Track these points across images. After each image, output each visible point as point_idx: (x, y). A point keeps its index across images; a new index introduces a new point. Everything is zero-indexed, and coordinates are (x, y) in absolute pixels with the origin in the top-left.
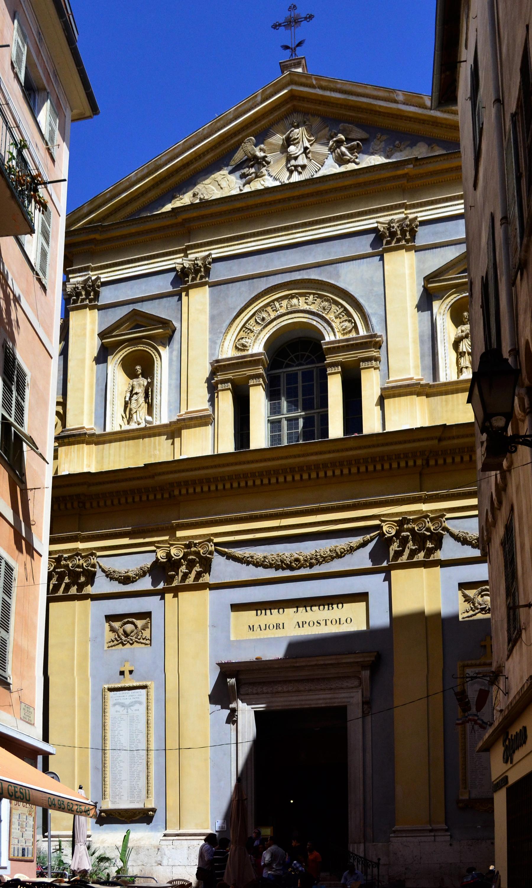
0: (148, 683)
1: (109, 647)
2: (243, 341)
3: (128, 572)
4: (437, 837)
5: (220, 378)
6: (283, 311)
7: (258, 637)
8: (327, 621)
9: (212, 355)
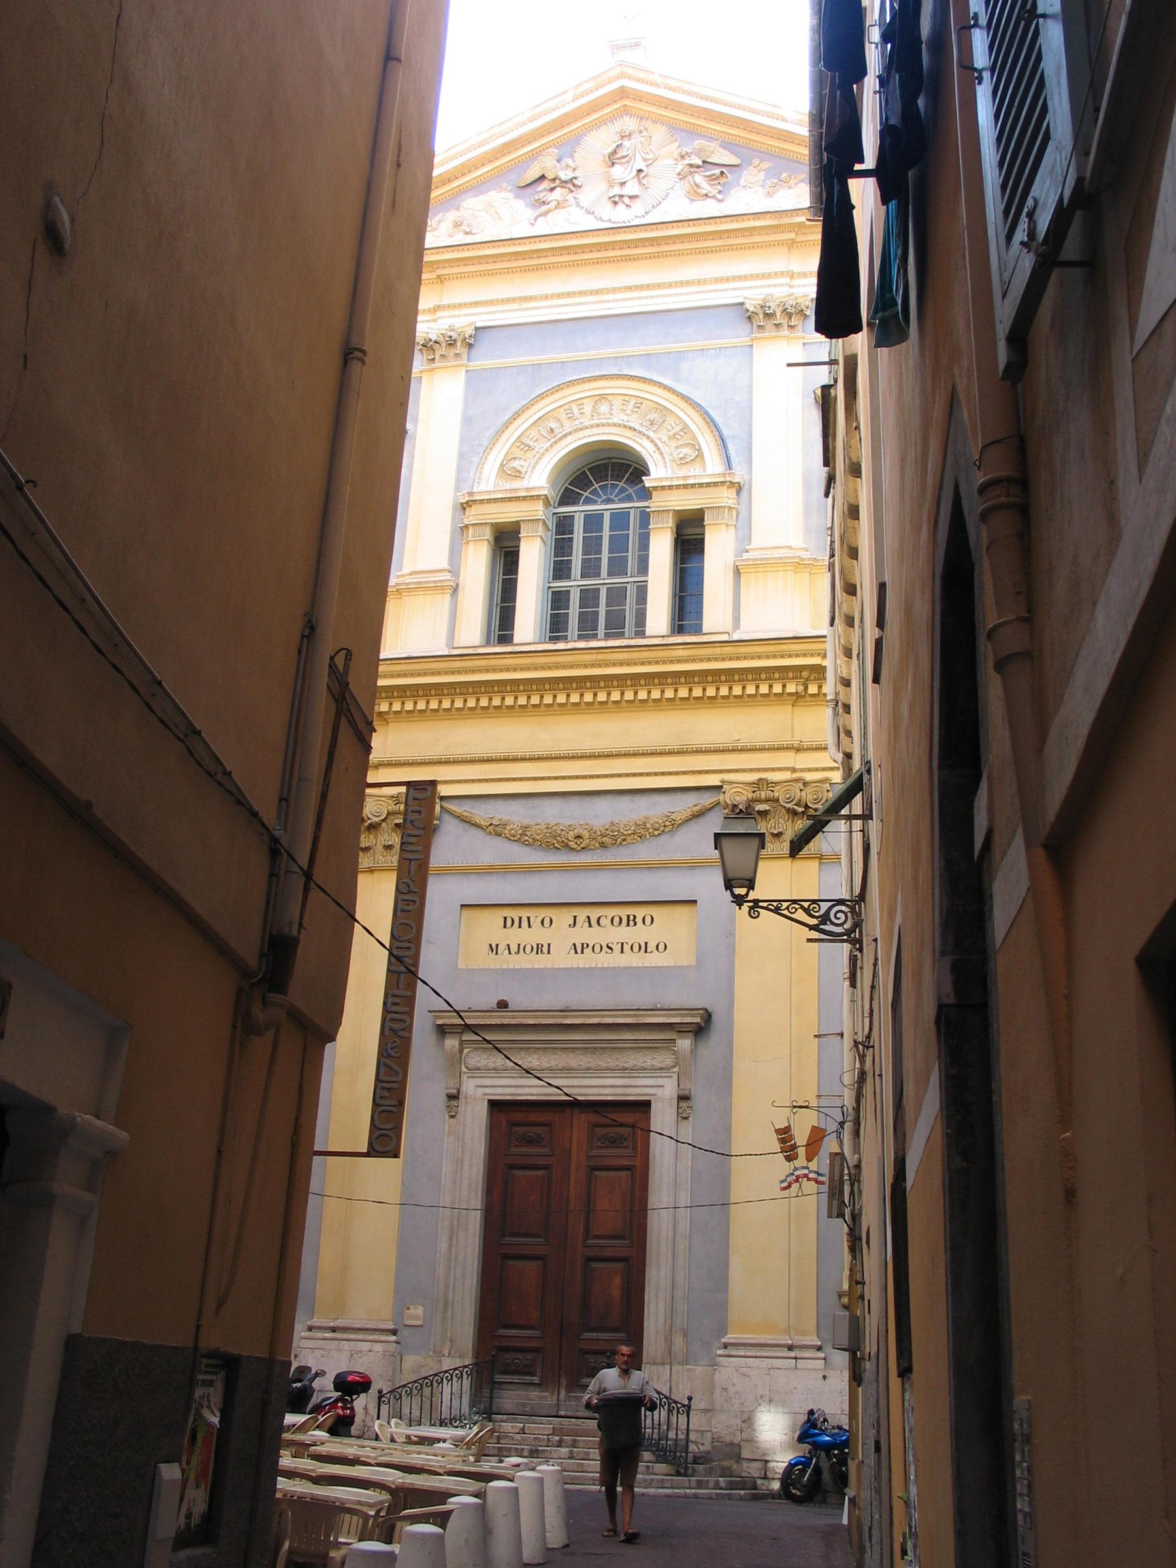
2: (516, 464)
4: (801, 1364)
7: (505, 966)
9: (459, 481)
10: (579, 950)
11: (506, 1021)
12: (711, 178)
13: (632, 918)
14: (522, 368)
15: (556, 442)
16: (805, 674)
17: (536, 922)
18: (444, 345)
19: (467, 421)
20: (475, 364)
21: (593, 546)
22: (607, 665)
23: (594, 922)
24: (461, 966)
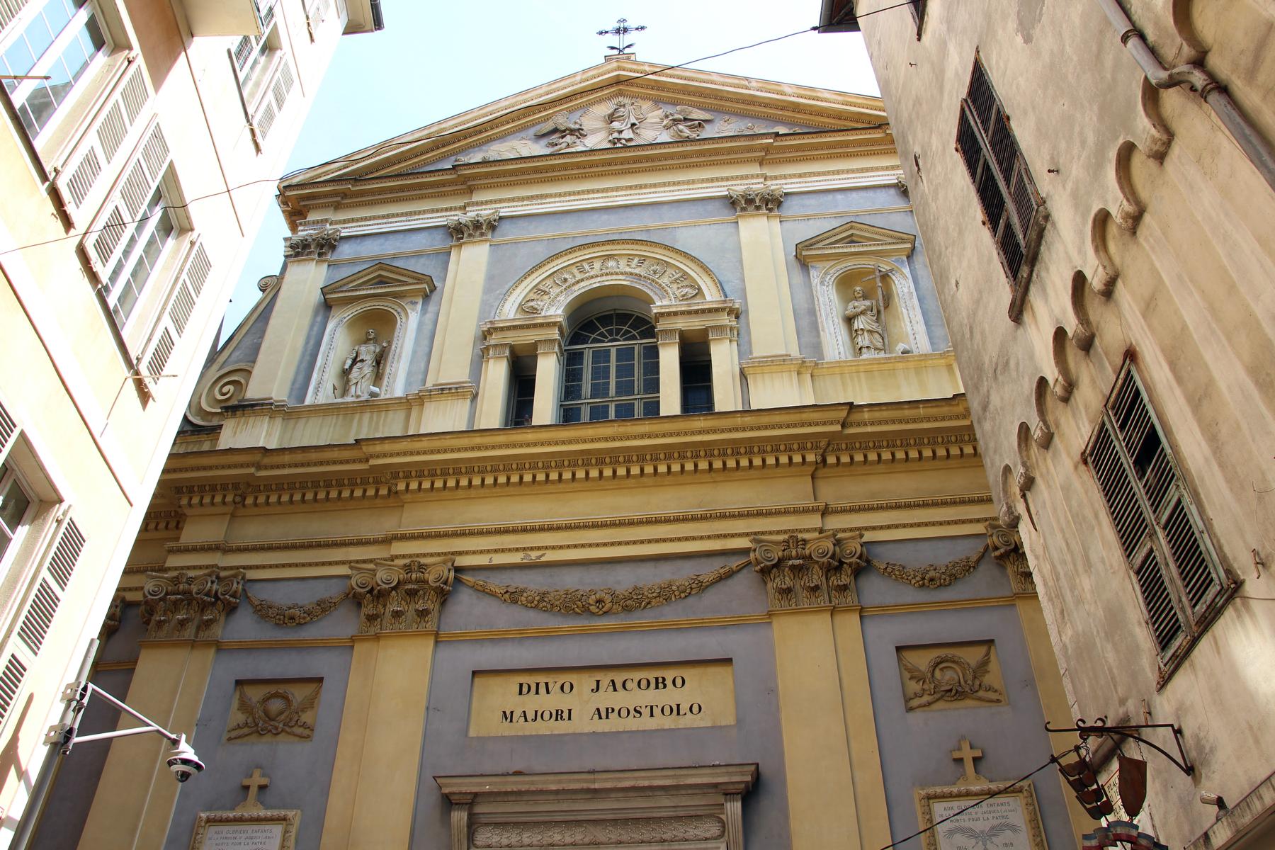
0: (290, 814)
1: (230, 739)
5: (493, 342)
6: (592, 273)
7: (520, 734)
9: (485, 306)
10: (603, 714)
12: (691, 127)
17: (555, 689)
19: (490, 278)
20: (497, 238)
21: (600, 373)
22: (628, 438)
23: (619, 686)
24: (472, 733)
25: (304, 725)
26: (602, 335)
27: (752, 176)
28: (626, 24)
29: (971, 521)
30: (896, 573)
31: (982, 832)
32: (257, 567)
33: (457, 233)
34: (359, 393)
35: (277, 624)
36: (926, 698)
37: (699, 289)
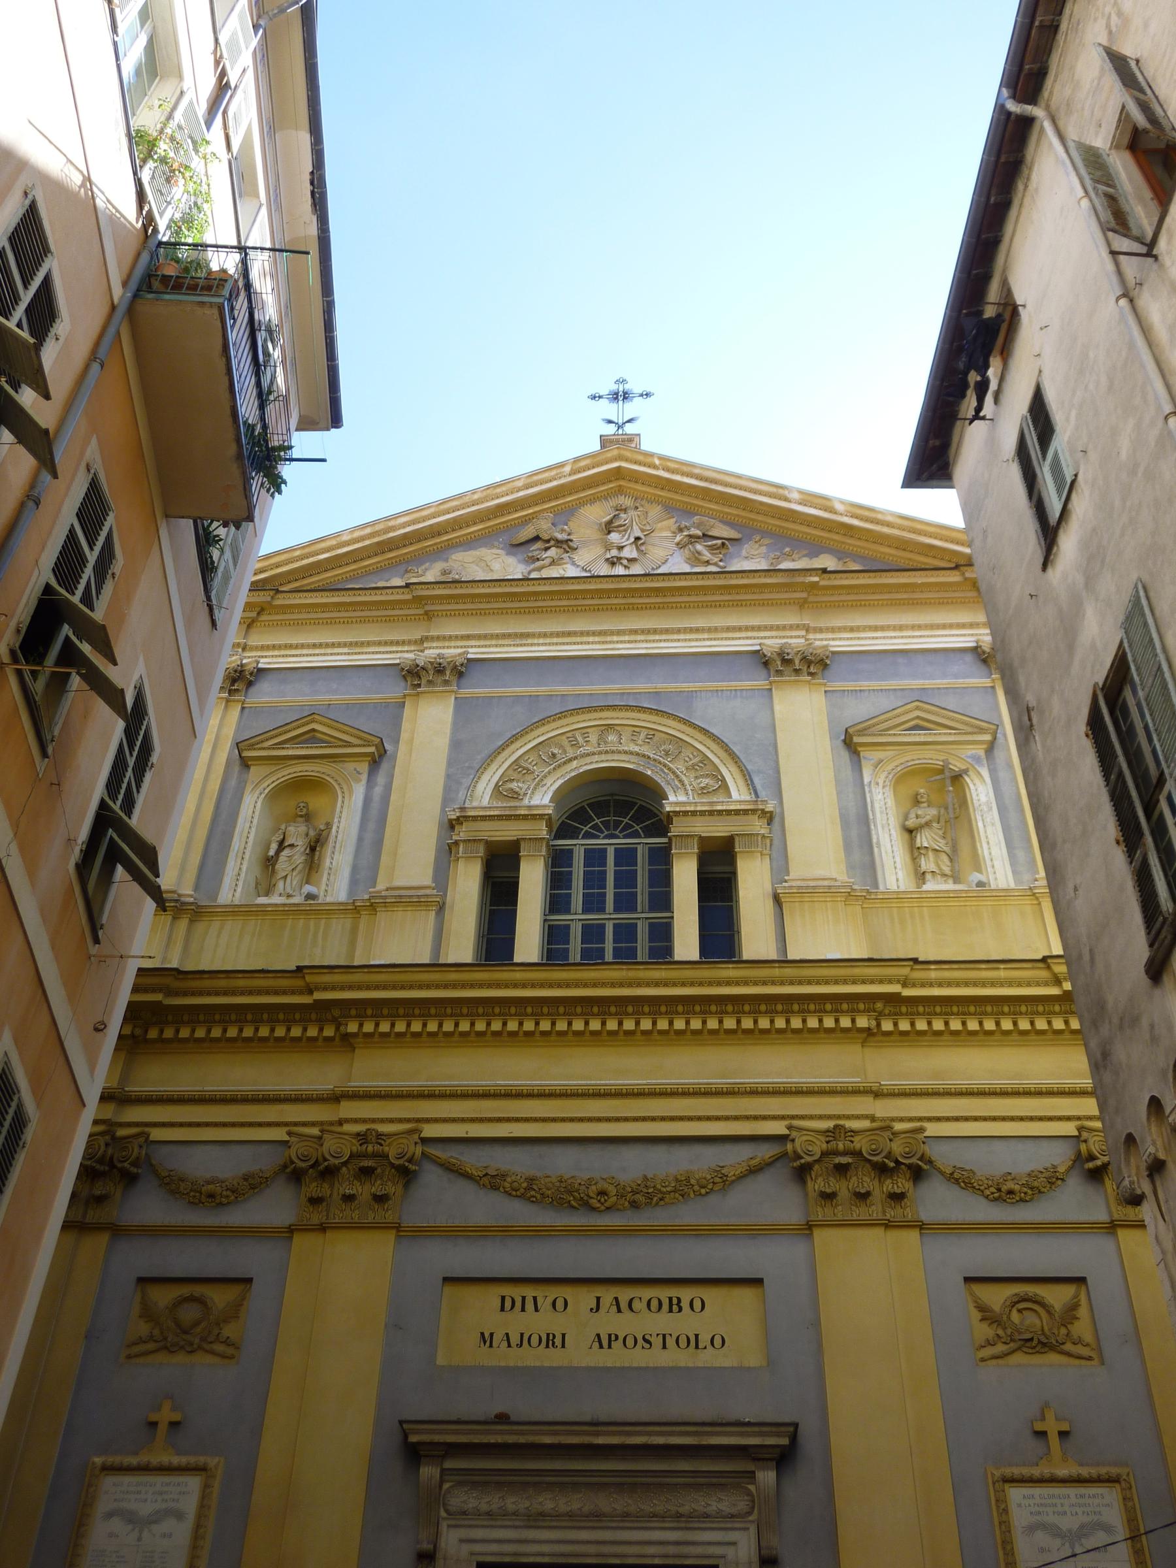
0: (212, 1461)
2: (514, 785)
3: (212, 1183)
5: (463, 836)
6: (589, 749)
7: (503, 1364)
8: (668, 1337)
10: (605, 1343)
11: (511, 1439)
12: (711, 548)
13: (675, 1301)
14: (518, 699)
15: (559, 766)
16: (879, 1005)
17: (544, 1305)
18: (431, 672)
19: (456, 745)
20: (466, 692)
21: (594, 880)
23: (624, 1305)
24: (441, 1361)
25: (227, 1342)
26: (595, 827)
27: (791, 627)
28: (627, 387)
29: (1060, 1119)
30: (962, 1180)
31: (1070, 1531)
32: (164, 1125)
33: (413, 675)
34: (289, 890)
35: (190, 1202)
36: (1000, 1348)
37: (723, 780)
